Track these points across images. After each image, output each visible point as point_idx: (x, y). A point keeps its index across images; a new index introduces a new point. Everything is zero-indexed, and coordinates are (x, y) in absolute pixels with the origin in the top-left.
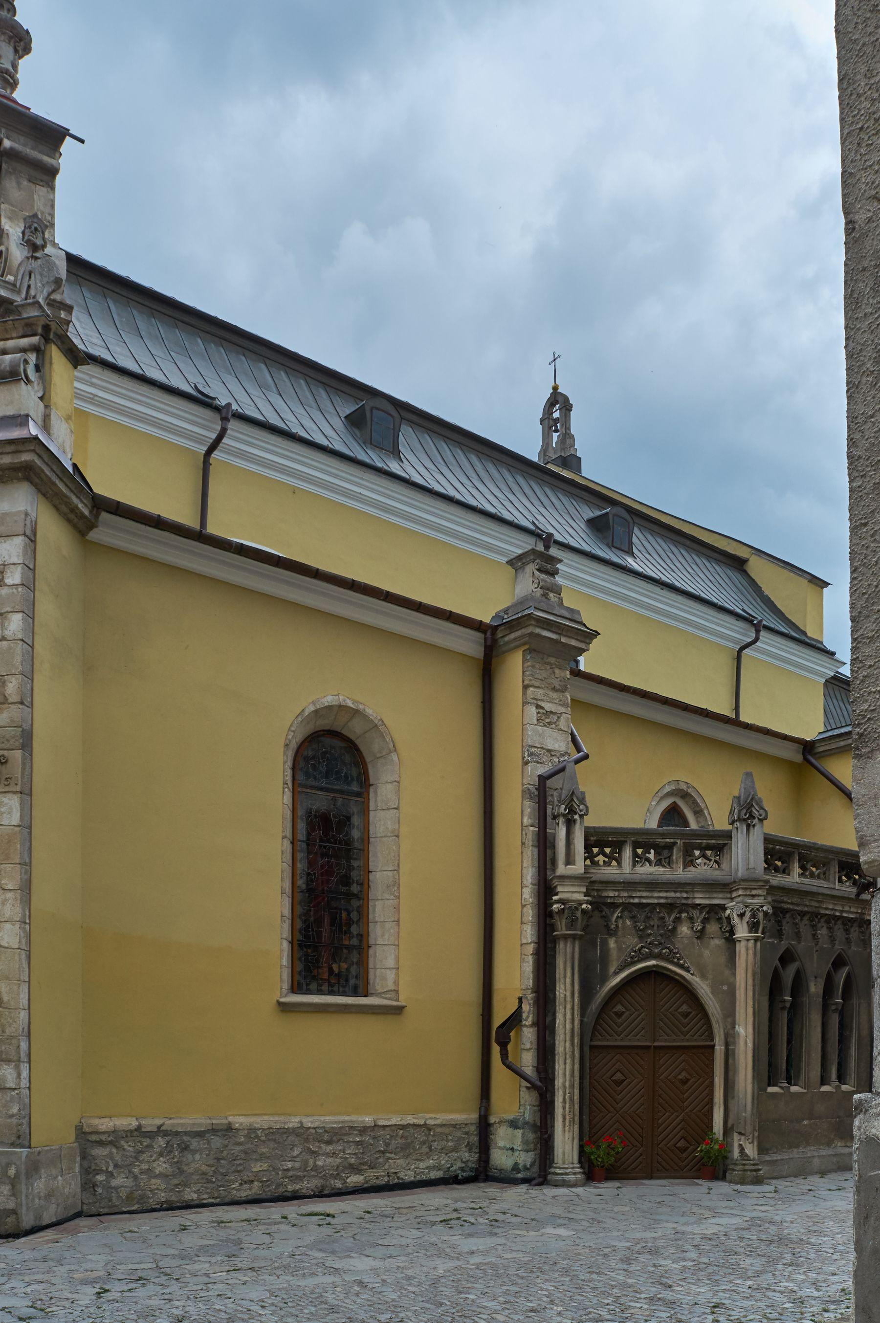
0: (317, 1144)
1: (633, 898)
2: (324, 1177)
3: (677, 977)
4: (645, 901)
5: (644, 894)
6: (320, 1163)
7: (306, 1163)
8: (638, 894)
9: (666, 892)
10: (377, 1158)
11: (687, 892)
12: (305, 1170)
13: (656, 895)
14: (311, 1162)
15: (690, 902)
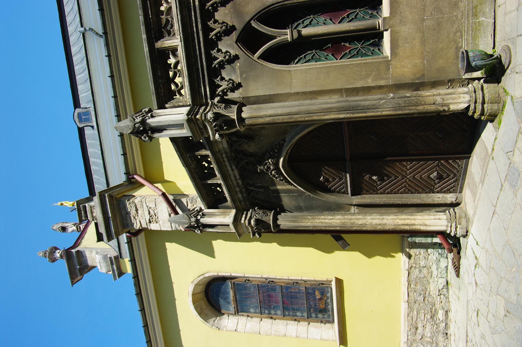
0: (417, 335)
1: (238, 183)
2: (438, 332)
3: (289, 151)
4: (238, 177)
5: (233, 178)
6: (429, 335)
7: (428, 342)
8: (234, 182)
9: (226, 167)
10: (429, 302)
11: (222, 155)
12: (432, 343)
13: (231, 172)
14: (428, 339)
15: (228, 150)
